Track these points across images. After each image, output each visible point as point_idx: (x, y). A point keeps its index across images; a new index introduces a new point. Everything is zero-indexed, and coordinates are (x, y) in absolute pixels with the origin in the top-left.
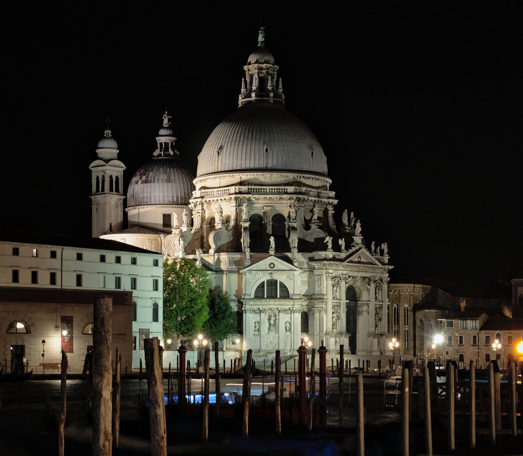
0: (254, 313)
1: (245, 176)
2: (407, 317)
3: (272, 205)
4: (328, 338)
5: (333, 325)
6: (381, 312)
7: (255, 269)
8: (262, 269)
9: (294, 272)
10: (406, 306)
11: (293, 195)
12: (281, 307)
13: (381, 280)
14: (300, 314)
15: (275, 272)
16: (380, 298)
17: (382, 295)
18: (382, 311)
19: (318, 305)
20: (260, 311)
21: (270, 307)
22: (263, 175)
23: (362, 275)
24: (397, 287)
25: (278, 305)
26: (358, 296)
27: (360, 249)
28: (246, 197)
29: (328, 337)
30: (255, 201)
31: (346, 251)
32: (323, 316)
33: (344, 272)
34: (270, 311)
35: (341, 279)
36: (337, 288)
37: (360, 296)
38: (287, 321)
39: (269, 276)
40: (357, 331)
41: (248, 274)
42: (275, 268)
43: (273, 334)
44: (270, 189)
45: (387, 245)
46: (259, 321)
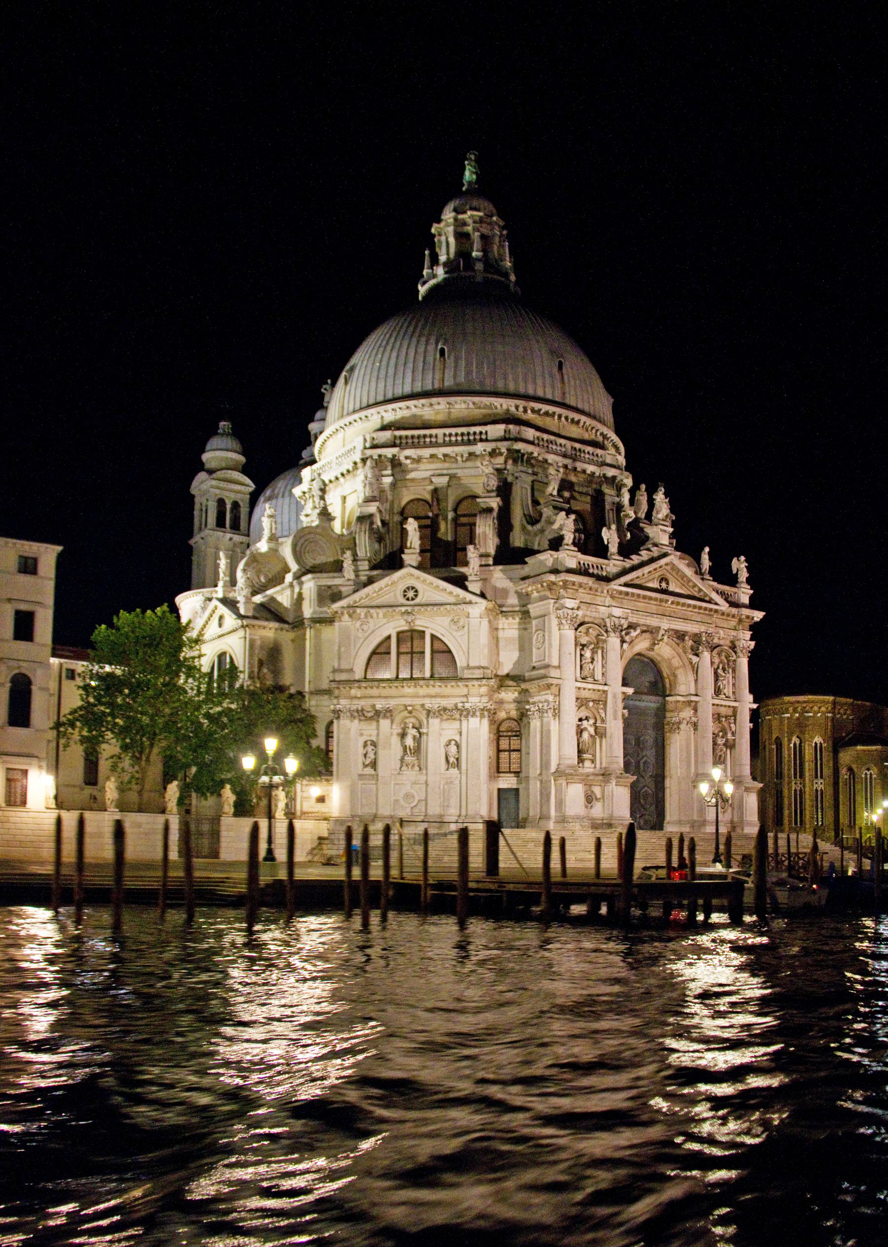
0: (363, 718)
1: (392, 413)
2: (821, 765)
3: (450, 472)
4: (561, 784)
5: (580, 752)
6: (733, 725)
7: (363, 602)
8: (385, 604)
9: (469, 609)
10: (818, 739)
11: (499, 444)
12: (434, 700)
13: (733, 647)
14: (486, 722)
15: (416, 608)
16: (728, 690)
17: (734, 685)
18: (735, 723)
19: (541, 698)
20: (378, 715)
21: (404, 703)
22: (431, 405)
23: (673, 627)
24: (798, 702)
25: (424, 697)
26: (668, 686)
27: (665, 555)
28: (385, 456)
29: (562, 782)
30: (410, 466)
31: (622, 558)
32: (549, 723)
33: (617, 612)
34: (406, 713)
35: (607, 631)
36: (594, 652)
37: (673, 685)
38: (450, 741)
39: (403, 622)
40: (667, 773)
41: (346, 617)
42: (417, 601)
43: (410, 774)
44: (445, 435)
45: (746, 561)
46: (374, 739)
